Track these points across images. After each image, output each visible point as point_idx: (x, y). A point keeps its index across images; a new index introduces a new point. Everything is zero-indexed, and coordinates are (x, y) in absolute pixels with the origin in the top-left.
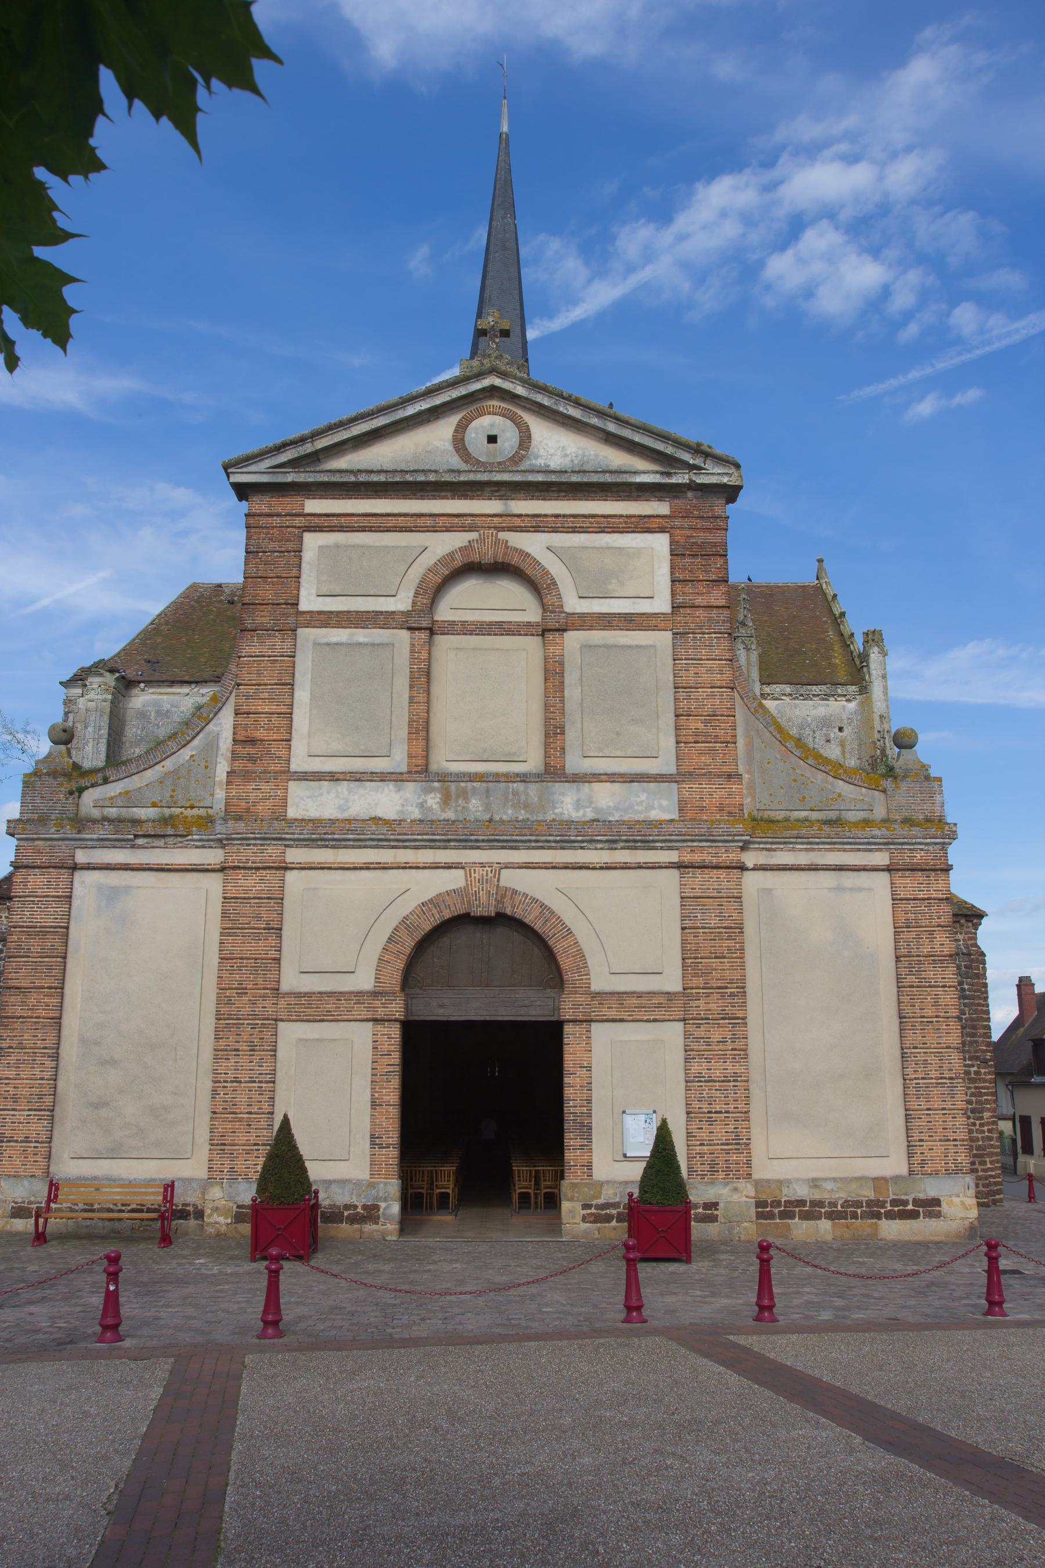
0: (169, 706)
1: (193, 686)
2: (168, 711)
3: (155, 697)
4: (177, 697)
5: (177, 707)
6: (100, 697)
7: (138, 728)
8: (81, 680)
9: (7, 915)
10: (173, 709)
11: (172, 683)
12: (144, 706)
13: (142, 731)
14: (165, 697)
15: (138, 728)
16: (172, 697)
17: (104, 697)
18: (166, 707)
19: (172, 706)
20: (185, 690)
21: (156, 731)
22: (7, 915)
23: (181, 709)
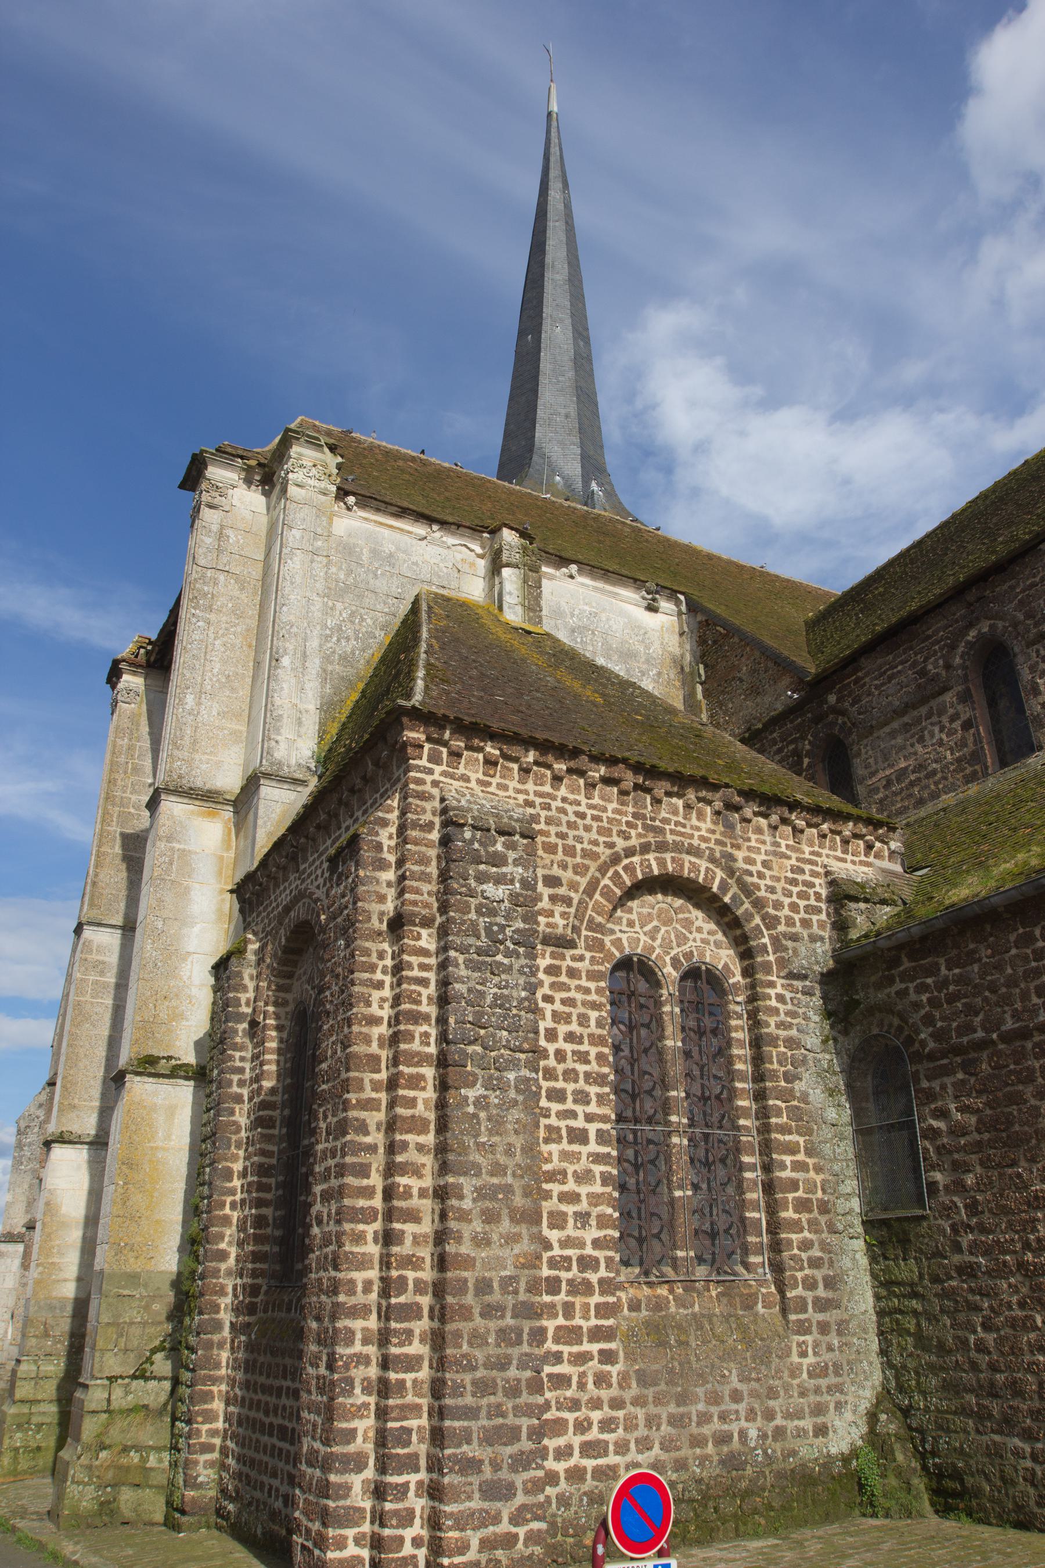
0: (393, 549)
1: (435, 527)
2: (391, 555)
3: (370, 527)
4: (406, 538)
5: (405, 552)
6: (316, 483)
7: (340, 568)
8: (242, 457)
9: (481, 776)
10: (401, 555)
11: (402, 512)
12: (349, 535)
13: (348, 575)
14: (386, 532)
15: (340, 568)
16: (397, 536)
17: (323, 485)
18: (388, 548)
19: (398, 549)
20: (420, 529)
21: (372, 582)
22: (481, 776)
23: (414, 559)
